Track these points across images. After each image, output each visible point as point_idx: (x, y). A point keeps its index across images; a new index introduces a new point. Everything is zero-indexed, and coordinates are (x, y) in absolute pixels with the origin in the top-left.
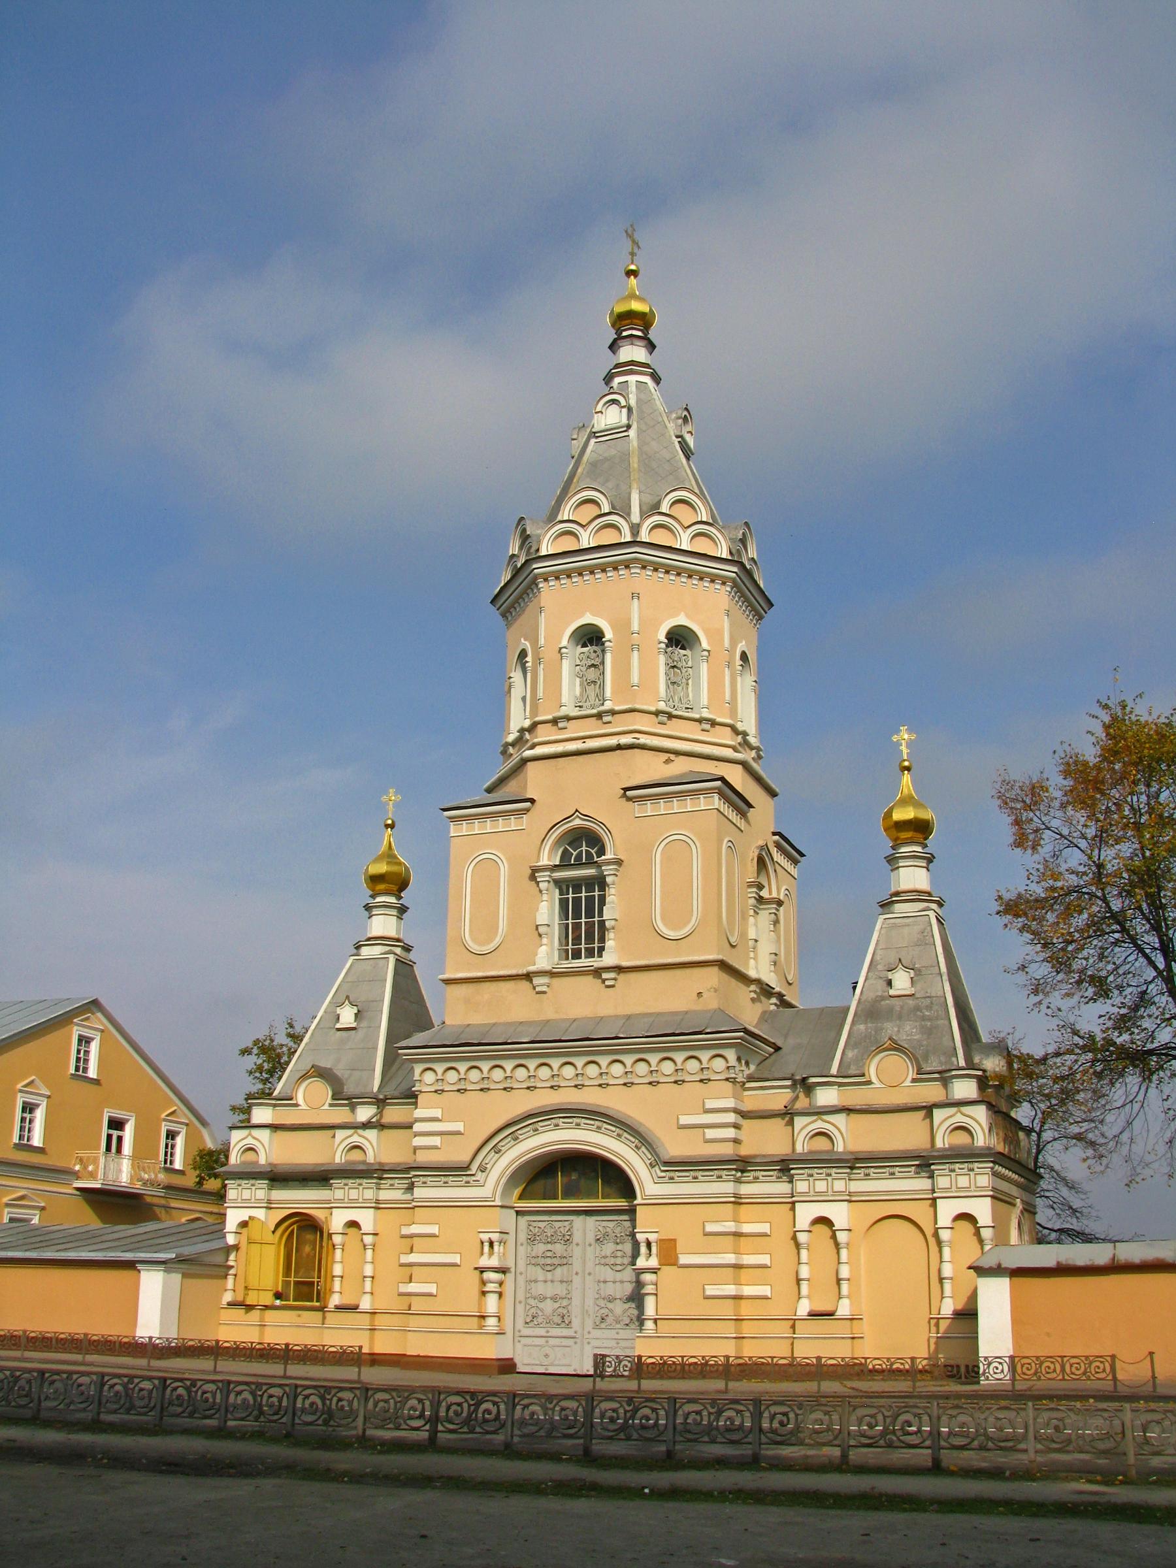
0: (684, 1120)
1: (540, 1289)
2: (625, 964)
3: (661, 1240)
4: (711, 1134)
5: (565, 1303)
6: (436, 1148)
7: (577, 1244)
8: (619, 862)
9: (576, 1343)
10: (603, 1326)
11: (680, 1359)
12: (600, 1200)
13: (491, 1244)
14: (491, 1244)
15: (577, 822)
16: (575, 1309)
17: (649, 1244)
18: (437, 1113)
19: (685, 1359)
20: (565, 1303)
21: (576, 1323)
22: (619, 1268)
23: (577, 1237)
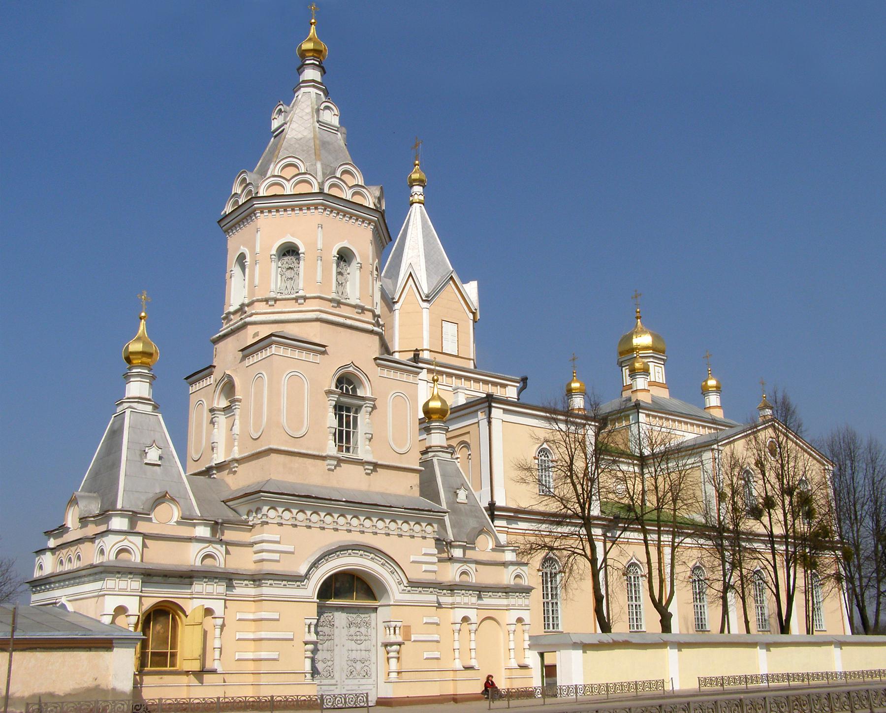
0: (412, 558)
1: (354, 655)
2: (380, 462)
3: (404, 626)
4: (425, 567)
5: (330, 663)
6: (278, 561)
7: (337, 627)
8: (374, 400)
9: (337, 688)
10: (351, 677)
11: (296, 697)
12: (354, 600)
13: (309, 626)
14: (309, 626)
15: (351, 369)
16: (337, 668)
17: (395, 628)
18: (277, 538)
19: (299, 697)
20: (330, 663)
21: (337, 675)
22: (359, 642)
23: (336, 623)
